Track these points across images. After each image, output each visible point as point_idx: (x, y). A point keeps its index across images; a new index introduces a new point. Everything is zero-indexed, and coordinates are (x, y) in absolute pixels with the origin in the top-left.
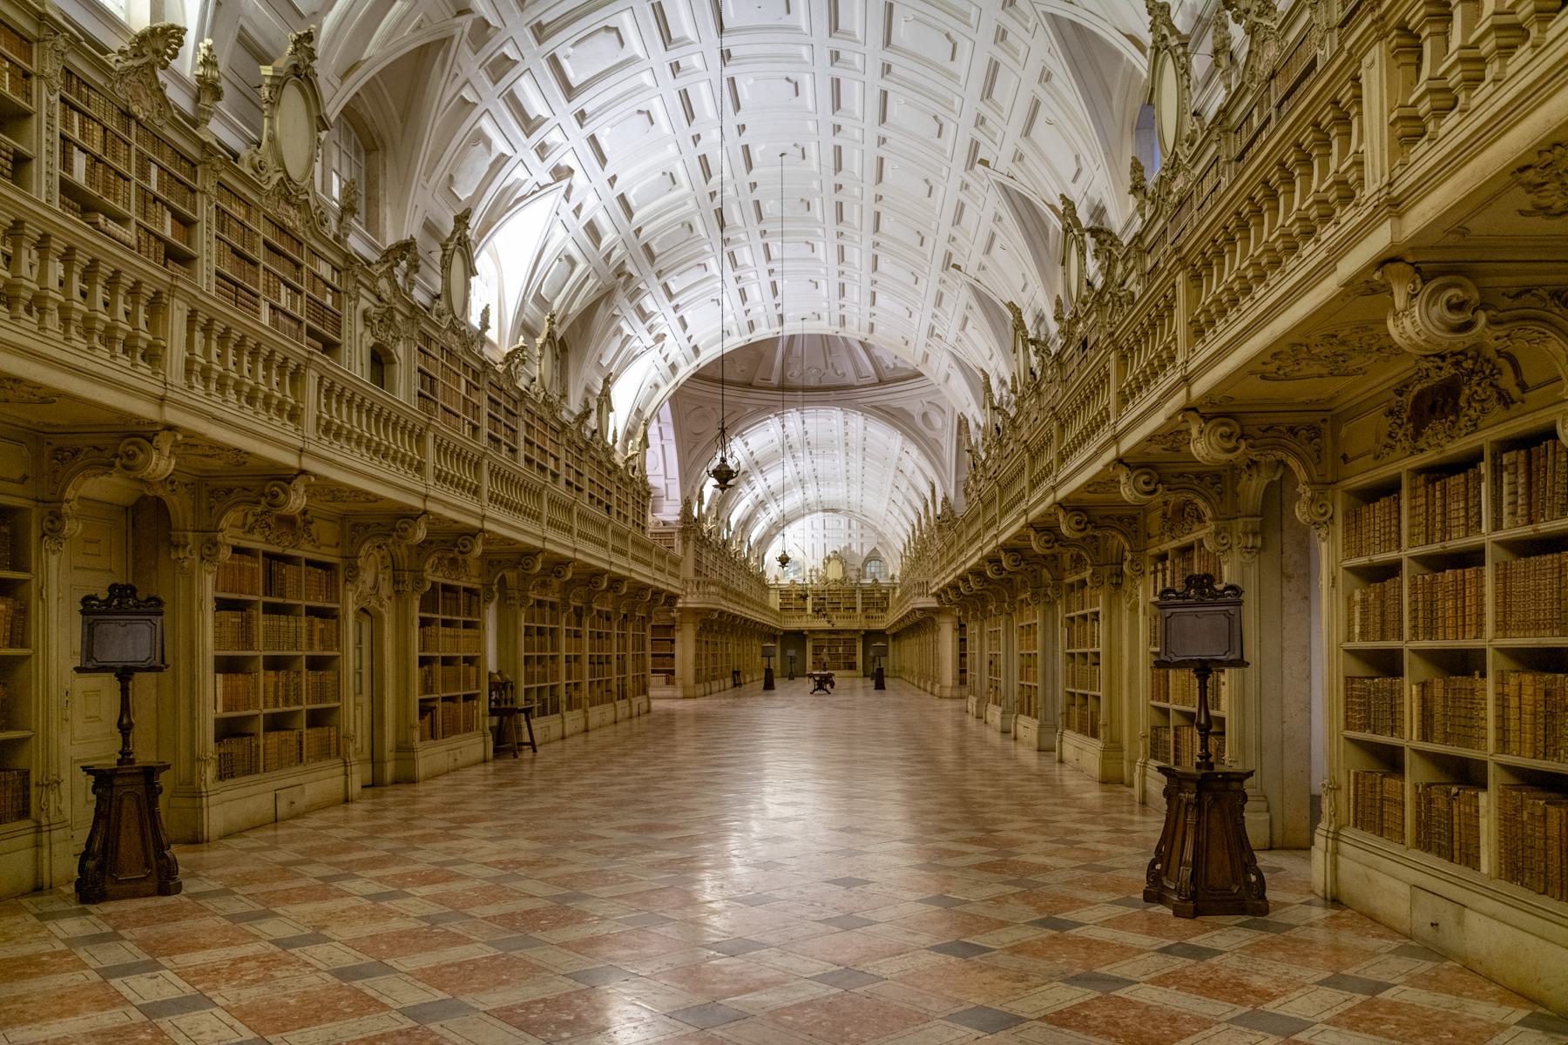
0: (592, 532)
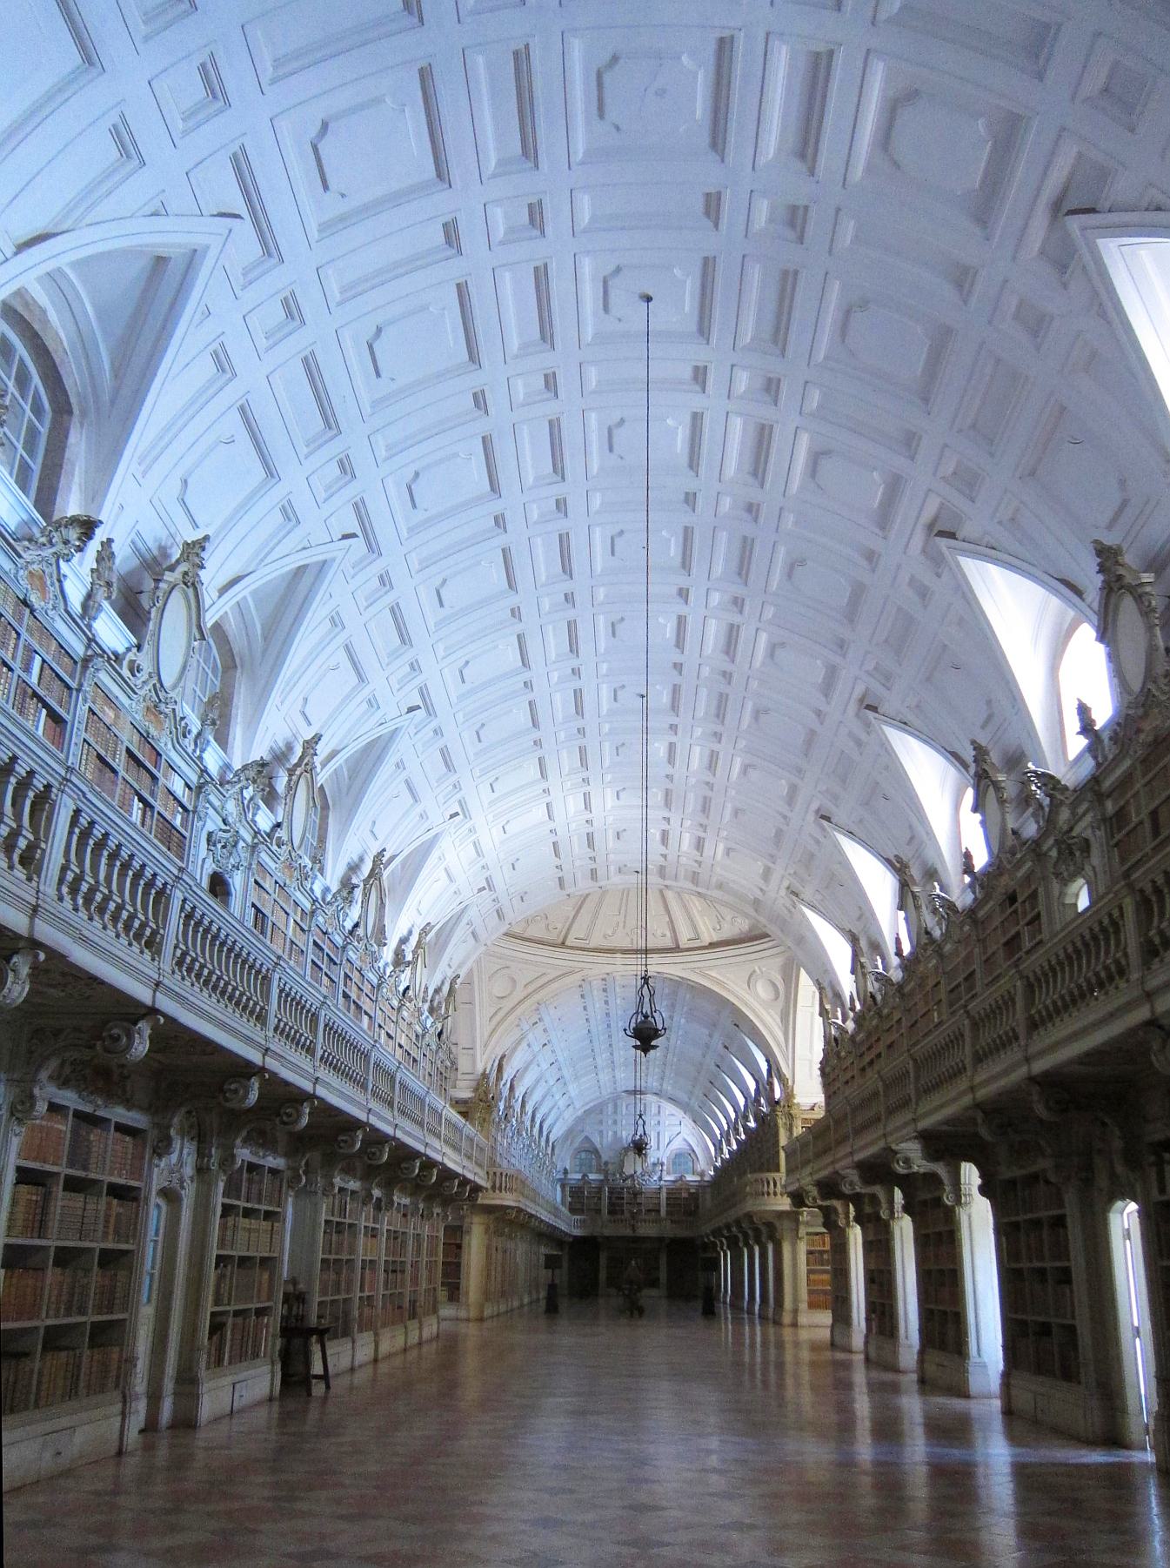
0: (410, 1106)
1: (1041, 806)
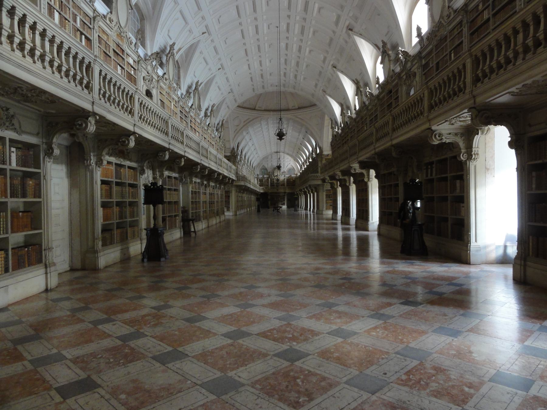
1: (402, 62)
